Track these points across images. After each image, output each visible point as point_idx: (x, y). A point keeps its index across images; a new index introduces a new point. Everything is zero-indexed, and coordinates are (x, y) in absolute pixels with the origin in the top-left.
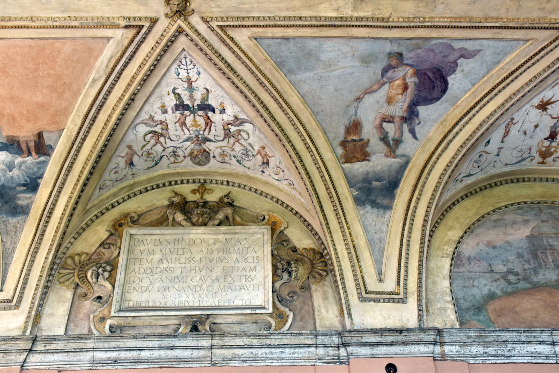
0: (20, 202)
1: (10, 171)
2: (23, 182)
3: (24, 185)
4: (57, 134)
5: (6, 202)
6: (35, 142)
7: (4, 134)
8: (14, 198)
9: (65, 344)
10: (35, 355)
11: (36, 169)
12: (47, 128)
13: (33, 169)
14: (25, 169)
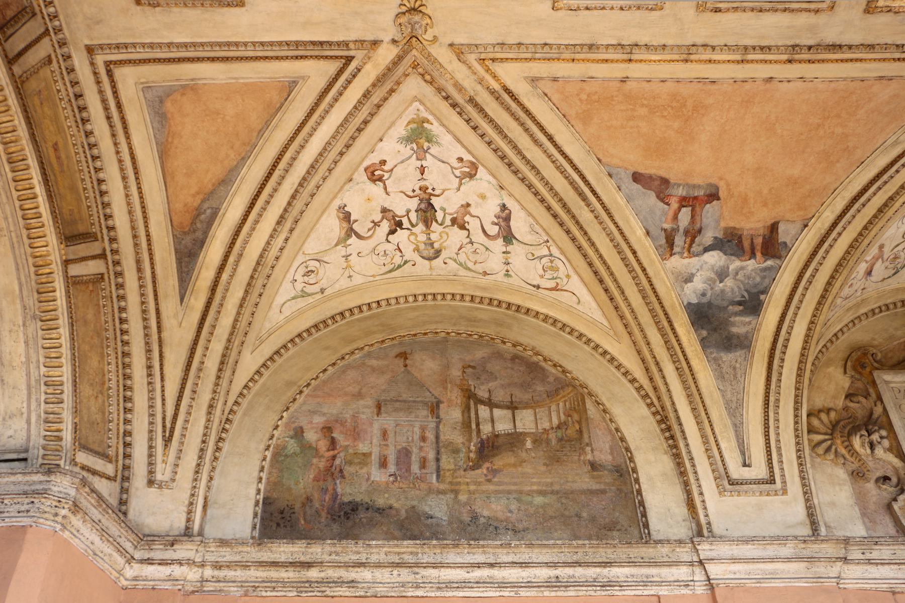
0: (735, 330)
1: (721, 282)
2: (738, 299)
3: (740, 303)
4: (799, 225)
5: (715, 330)
6: (764, 238)
7: (723, 224)
8: (726, 323)
9: (893, 552)
10: (851, 567)
11: (758, 279)
12: (788, 216)
13: (754, 278)
14: (743, 279)
